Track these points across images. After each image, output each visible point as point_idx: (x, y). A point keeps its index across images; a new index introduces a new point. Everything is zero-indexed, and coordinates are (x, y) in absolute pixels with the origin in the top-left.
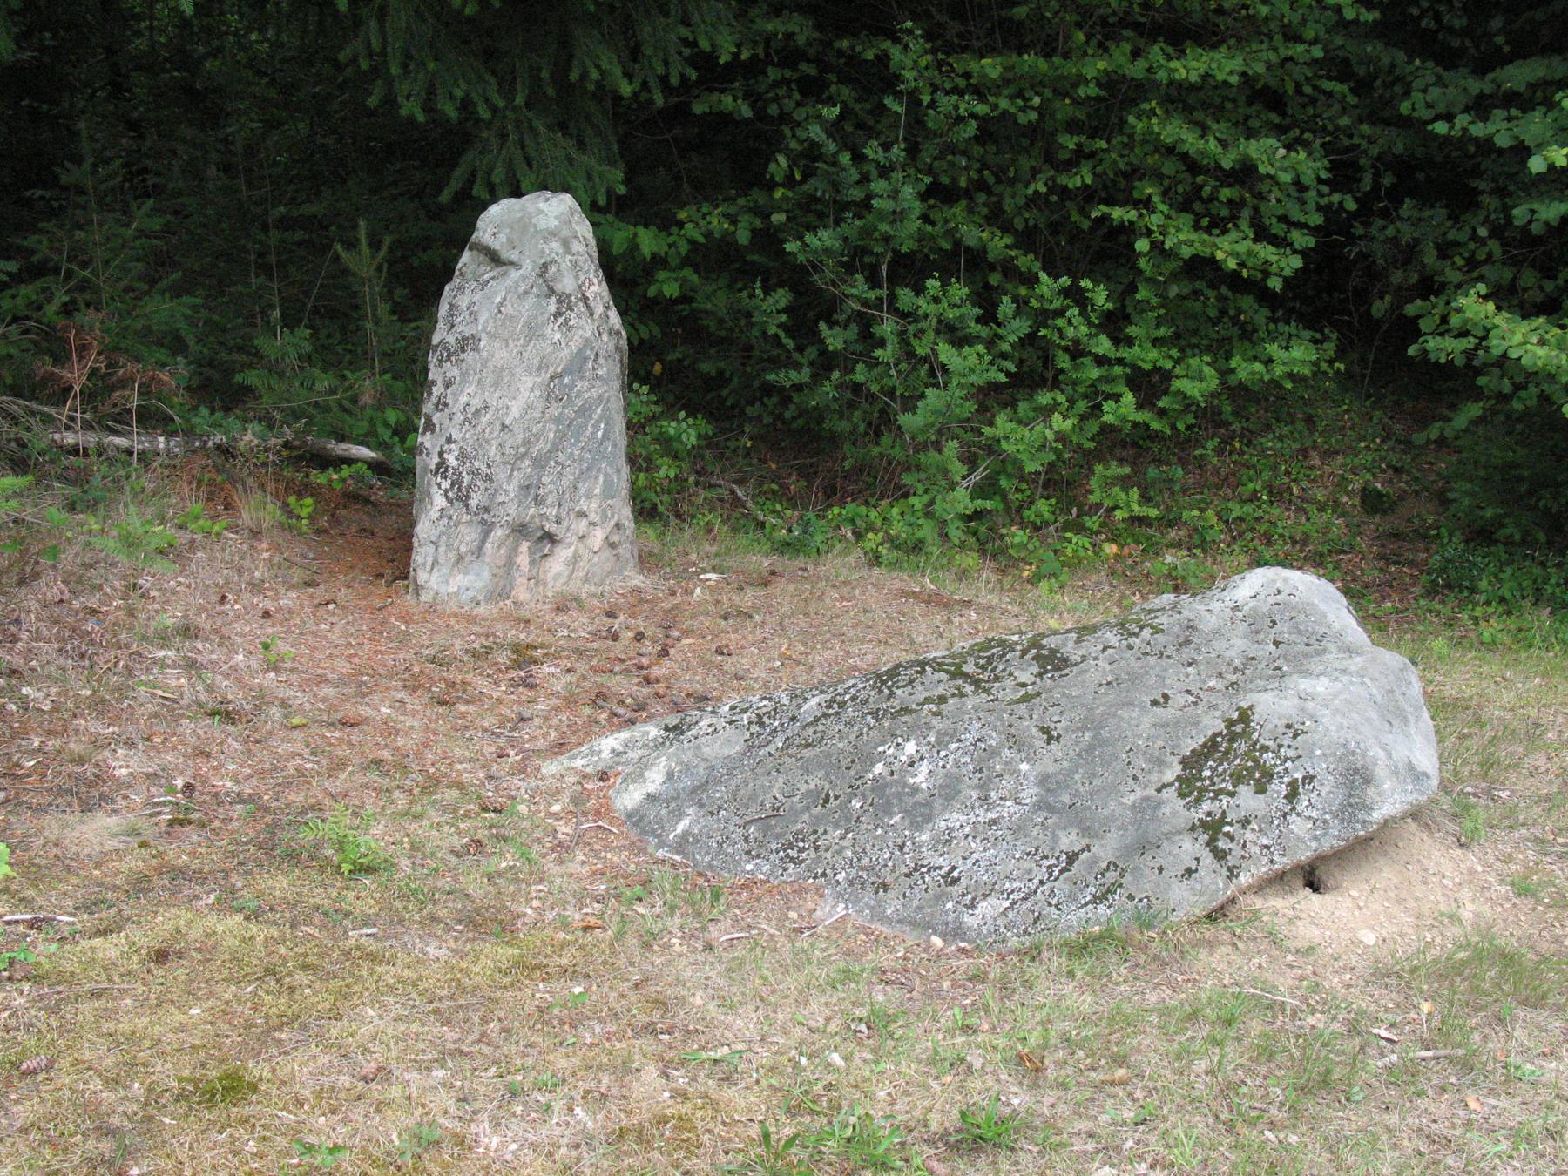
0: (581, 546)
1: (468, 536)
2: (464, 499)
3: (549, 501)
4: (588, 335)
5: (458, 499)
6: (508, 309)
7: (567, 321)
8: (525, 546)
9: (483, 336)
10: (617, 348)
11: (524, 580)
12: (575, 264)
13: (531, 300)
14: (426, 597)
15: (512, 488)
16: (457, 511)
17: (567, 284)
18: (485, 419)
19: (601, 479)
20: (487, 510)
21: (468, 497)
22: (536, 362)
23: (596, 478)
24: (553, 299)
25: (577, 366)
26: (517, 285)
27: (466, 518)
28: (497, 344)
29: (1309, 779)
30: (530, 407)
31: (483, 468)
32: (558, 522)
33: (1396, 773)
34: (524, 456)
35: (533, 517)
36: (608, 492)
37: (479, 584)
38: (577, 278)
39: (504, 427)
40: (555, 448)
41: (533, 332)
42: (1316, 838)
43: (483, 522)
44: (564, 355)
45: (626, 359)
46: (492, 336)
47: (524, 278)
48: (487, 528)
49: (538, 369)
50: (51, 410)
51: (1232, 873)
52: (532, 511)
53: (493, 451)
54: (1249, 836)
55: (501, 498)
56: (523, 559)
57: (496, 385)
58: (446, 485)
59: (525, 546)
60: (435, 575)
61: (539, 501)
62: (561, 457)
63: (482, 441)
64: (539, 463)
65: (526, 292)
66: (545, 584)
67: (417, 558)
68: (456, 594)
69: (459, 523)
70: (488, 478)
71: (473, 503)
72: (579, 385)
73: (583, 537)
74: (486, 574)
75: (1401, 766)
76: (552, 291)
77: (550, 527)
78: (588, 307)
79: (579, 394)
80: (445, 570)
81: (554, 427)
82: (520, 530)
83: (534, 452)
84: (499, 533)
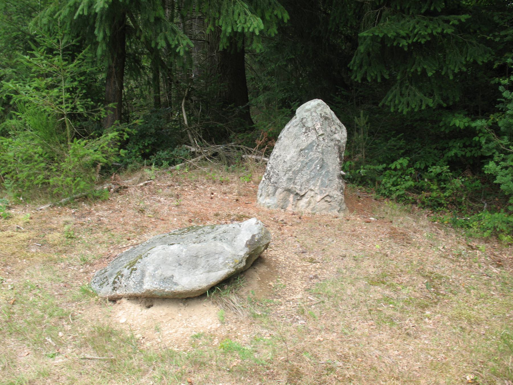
0: (312, 199)
1: (271, 189)
2: (270, 179)
3: (298, 184)
4: (314, 139)
5: (268, 179)
6: (290, 130)
7: (308, 135)
8: (292, 196)
9: (283, 136)
10: (335, 145)
11: (291, 205)
12: (312, 119)
13: (297, 128)
14: (258, 203)
15: (285, 178)
16: (267, 182)
17: (309, 124)
18: (279, 159)
19: (320, 181)
20: (276, 183)
21: (271, 179)
22: (296, 145)
23: (318, 181)
24: (304, 128)
25: (310, 147)
26: (294, 123)
27: (270, 184)
28: (286, 139)
29: (136, 269)
30: (293, 157)
31: (277, 172)
32: (301, 190)
33: (154, 276)
34: (290, 170)
35: (292, 188)
36: (323, 184)
37: (273, 203)
38: (313, 123)
39: (284, 162)
40: (300, 170)
41: (296, 137)
42: (134, 288)
43: (274, 186)
44: (304, 145)
45: (343, 149)
46: (285, 137)
47: (296, 122)
48: (276, 189)
49: (297, 147)
50: (250, 149)
51: (114, 289)
52: (292, 186)
53: (280, 167)
54: (123, 281)
55: (281, 181)
56: (291, 198)
57: (284, 150)
58: (266, 174)
59: (292, 196)
60: (261, 198)
61: (294, 183)
62: (303, 172)
63: (277, 165)
64: (296, 173)
65: (296, 126)
66: (298, 207)
67: (258, 193)
68: (264, 204)
69: (268, 185)
70: (278, 175)
71: (272, 180)
72: (311, 153)
73: (312, 197)
74: (276, 201)
75: (157, 275)
76: (304, 126)
77: (299, 192)
78: (316, 132)
79: (310, 156)
80: (264, 197)
81: (300, 164)
82: (289, 191)
83: (293, 169)
84: (280, 190)
